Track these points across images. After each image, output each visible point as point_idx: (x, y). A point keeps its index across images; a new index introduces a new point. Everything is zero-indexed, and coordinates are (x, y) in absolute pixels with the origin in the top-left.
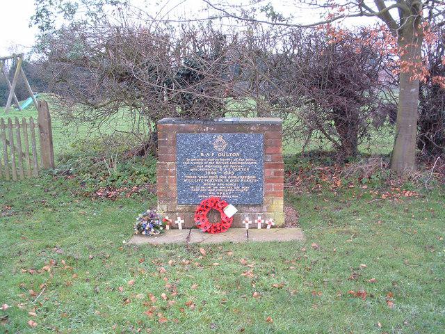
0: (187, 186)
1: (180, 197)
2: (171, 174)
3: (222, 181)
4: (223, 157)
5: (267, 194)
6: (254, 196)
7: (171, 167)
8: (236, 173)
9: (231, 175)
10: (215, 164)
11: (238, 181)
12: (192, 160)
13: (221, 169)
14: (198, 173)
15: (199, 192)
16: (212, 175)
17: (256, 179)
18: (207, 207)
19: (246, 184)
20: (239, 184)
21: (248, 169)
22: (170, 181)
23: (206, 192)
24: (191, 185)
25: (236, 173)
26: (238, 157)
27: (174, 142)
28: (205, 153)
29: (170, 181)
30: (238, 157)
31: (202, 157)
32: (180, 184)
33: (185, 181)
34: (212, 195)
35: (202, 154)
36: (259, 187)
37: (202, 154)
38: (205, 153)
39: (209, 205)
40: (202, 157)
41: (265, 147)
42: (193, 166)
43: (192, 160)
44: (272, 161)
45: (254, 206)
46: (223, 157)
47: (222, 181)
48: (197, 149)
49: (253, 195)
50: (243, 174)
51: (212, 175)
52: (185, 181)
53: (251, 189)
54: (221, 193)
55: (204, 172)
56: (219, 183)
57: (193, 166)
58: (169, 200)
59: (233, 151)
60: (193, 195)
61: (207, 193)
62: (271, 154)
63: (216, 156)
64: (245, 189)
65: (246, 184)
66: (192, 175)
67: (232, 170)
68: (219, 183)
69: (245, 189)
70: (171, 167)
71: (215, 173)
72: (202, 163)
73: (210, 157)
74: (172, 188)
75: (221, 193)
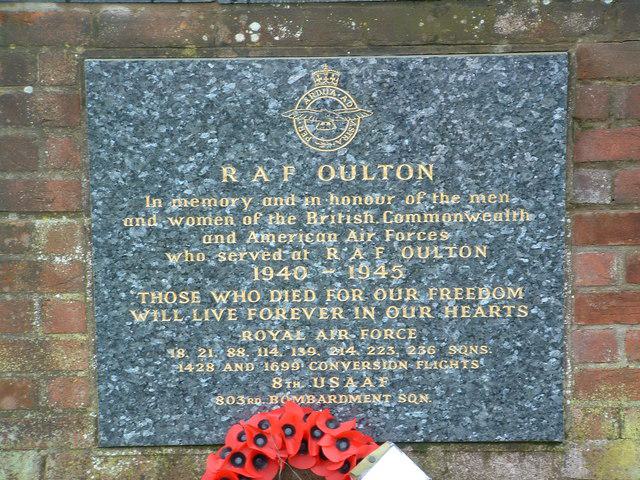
0: (151, 350)
1: (112, 405)
2: (61, 284)
3: (337, 313)
4: (341, 188)
5: (587, 383)
6: (517, 392)
7: (57, 243)
8: (415, 273)
9: (386, 282)
10: (300, 226)
11: (425, 313)
12: (176, 203)
13: (332, 254)
14: (212, 274)
15: (214, 378)
16: (282, 284)
17: (529, 300)
18: (260, 459)
19: (472, 332)
20: (430, 329)
21: (481, 251)
22: (57, 321)
23: (255, 375)
24: (171, 343)
25: (415, 273)
26: (428, 186)
27: (75, 104)
28: (246, 167)
29: (57, 321)
30: (428, 186)
31: (231, 189)
32: (110, 336)
33: (140, 318)
34: (288, 396)
35: (229, 173)
36: (542, 347)
37: (229, 173)
38: (246, 167)
39: (270, 452)
40: (231, 189)
41: (578, 122)
42: (175, 239)
43: (176, 203)
44: (616, 203)
45: (518, 446)
46: (341, 188)
47: (337, 313)
48: (203, 146)
49: (507, 388)
50: (455, 278)
51: (282, 284)
52: (140, 318)
53: (496, 357)
54: (334, 382)
55: (242, 271)
56: (328, 325)
57: (175, 239)
58: (49, 427)
59: (403, 154)
60: (181, 393)
61: (258, 385)
62: (608, 165)
63: (306, 183)
64: (467, 355)
65: (472, 332)
66: (177, 287)
67: (391, 253)
68: (328, 325)
69: (467, 355)
70: (57, 243)
71: (301, 273)
72: (230, 221)
73: (275, 186)
74: (65, 360)
75: (334, 382)
